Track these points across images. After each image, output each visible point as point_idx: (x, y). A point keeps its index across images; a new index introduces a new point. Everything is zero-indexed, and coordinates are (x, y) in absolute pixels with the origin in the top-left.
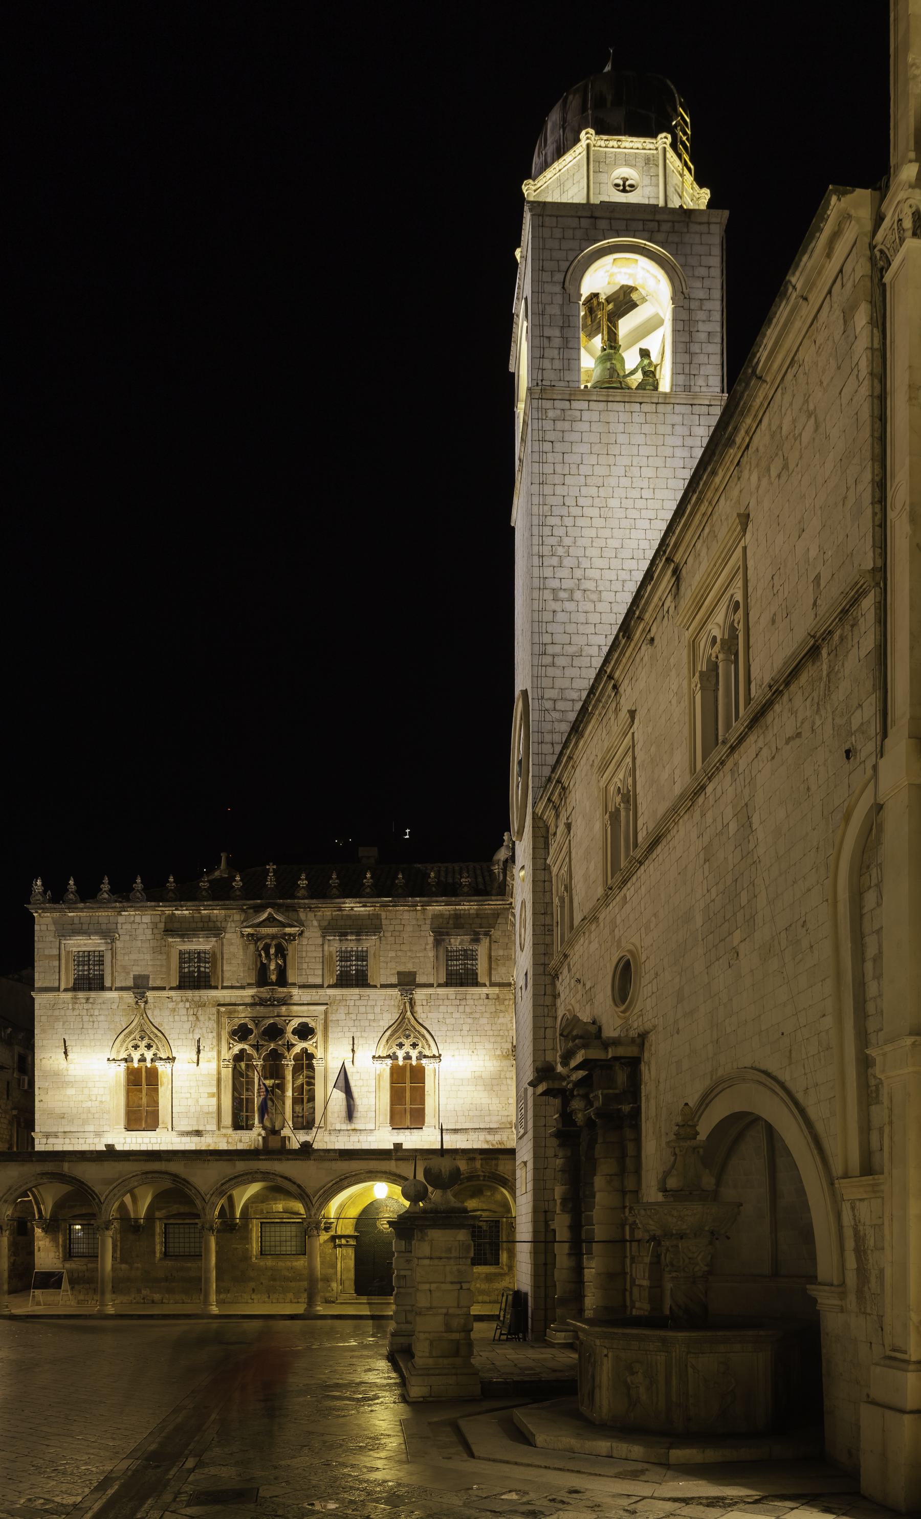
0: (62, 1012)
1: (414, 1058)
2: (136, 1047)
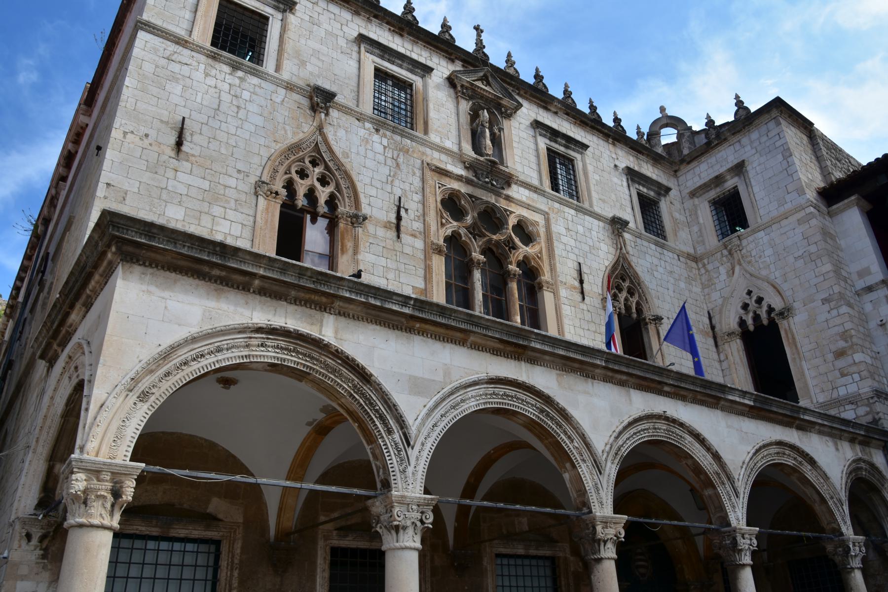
0: (186, 70)
1: (634, 310)
2: (303, 174)
